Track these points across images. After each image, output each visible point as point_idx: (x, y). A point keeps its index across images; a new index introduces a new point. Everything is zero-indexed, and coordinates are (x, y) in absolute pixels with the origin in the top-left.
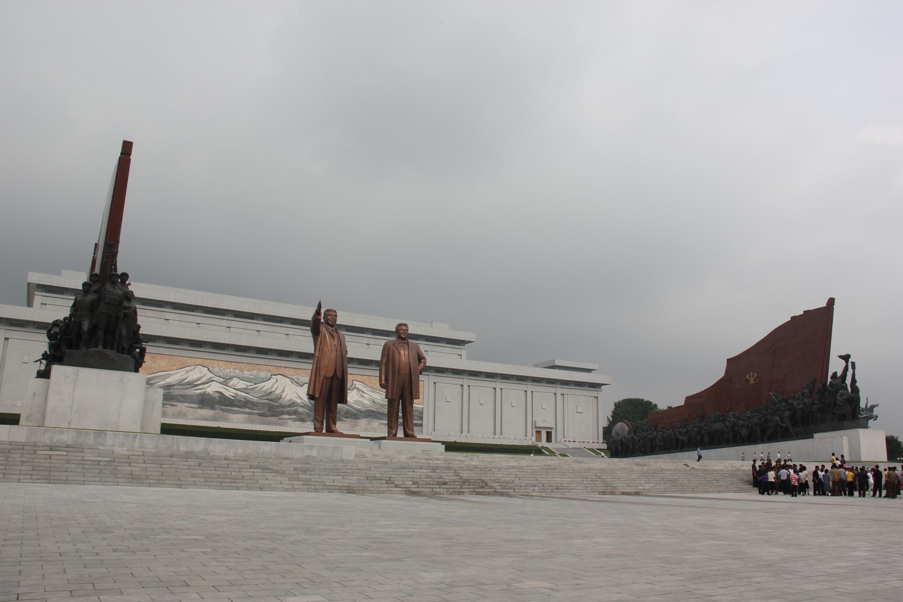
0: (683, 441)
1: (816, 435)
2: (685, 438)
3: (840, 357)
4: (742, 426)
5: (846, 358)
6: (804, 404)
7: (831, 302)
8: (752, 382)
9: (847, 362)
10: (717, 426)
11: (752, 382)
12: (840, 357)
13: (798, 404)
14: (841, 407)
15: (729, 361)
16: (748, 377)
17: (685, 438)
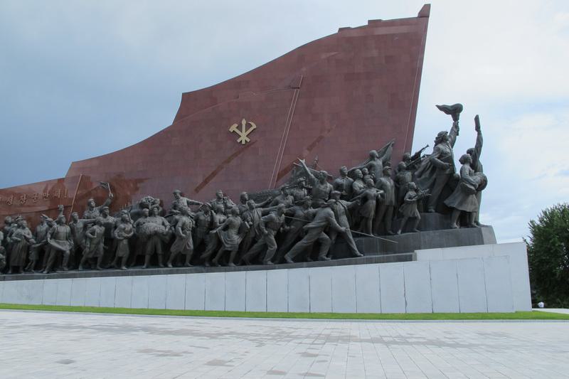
0: (62, 252)
1: (422, 254)
2: (66, 247)
3: (444, 109)
4: (226, 228)
5: (454, 111)
6: (382, 186)
7: (425, 13)
8: (244, 138)
9: (456, 118)
10: (155, 224)
11: (244, 138)
12: (444, 109)
13: (369, 186)
14: (440, 200)
15: (187, 98)
16: (233, 128)
17: (66, 247)
